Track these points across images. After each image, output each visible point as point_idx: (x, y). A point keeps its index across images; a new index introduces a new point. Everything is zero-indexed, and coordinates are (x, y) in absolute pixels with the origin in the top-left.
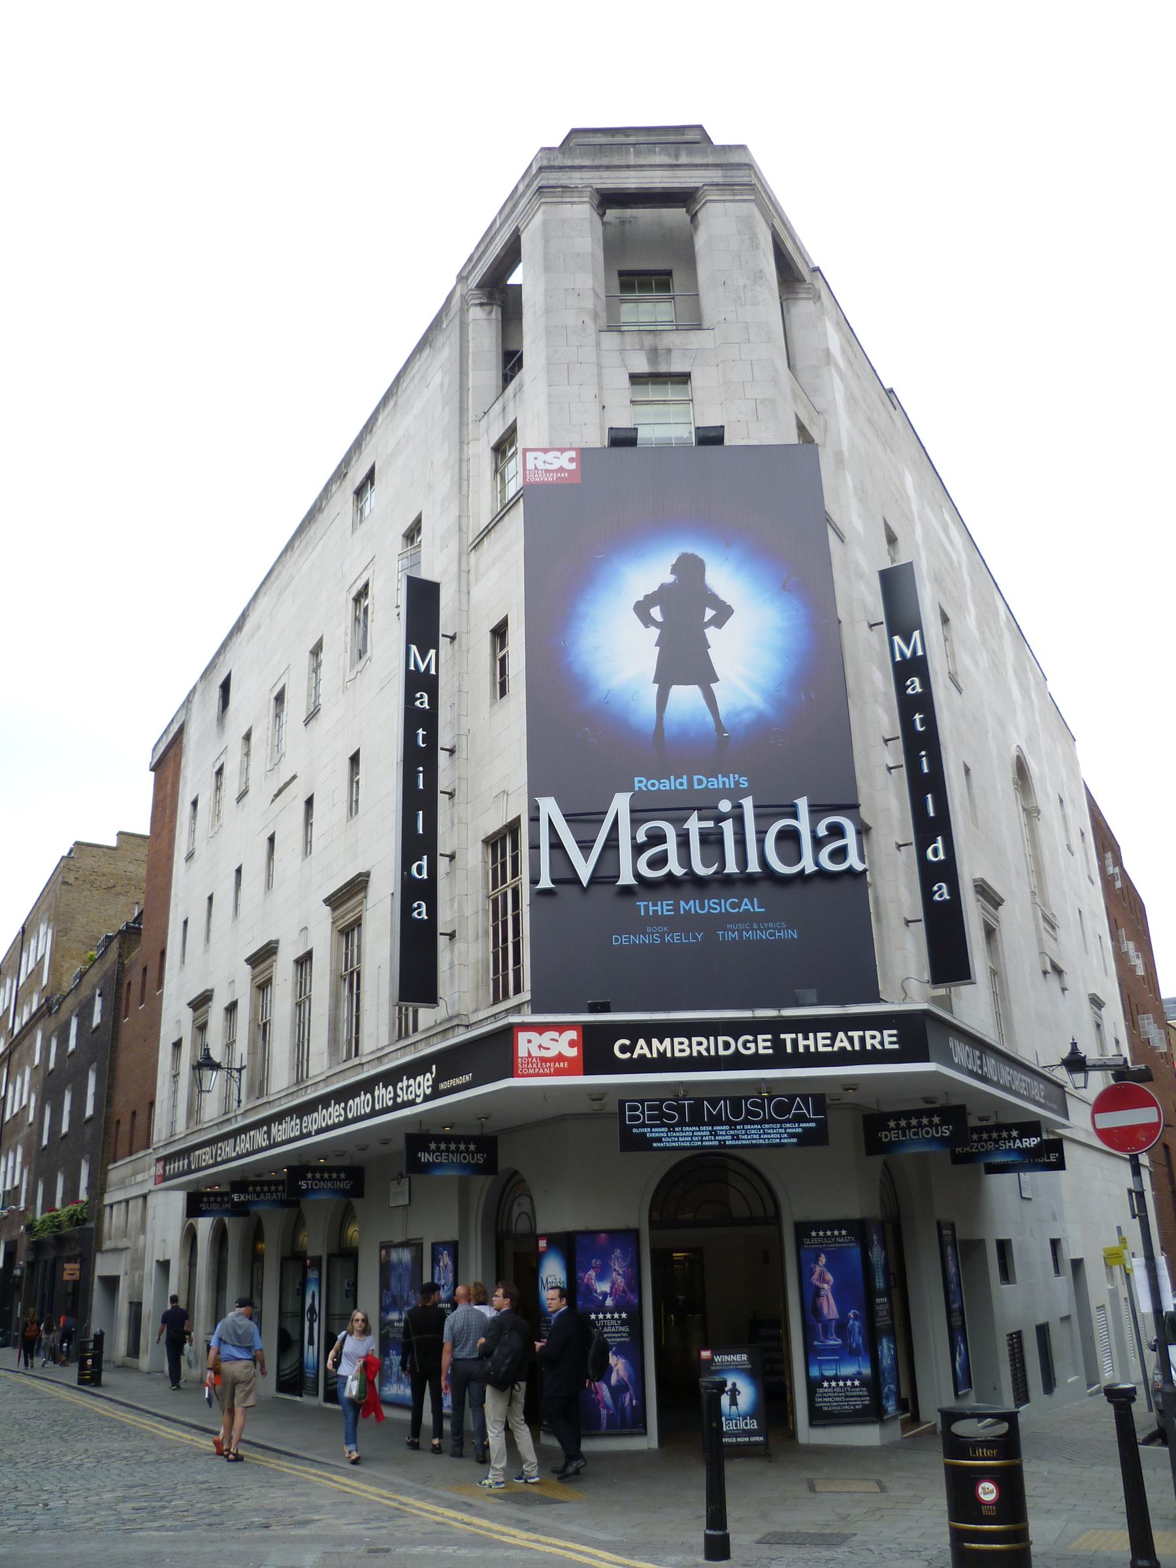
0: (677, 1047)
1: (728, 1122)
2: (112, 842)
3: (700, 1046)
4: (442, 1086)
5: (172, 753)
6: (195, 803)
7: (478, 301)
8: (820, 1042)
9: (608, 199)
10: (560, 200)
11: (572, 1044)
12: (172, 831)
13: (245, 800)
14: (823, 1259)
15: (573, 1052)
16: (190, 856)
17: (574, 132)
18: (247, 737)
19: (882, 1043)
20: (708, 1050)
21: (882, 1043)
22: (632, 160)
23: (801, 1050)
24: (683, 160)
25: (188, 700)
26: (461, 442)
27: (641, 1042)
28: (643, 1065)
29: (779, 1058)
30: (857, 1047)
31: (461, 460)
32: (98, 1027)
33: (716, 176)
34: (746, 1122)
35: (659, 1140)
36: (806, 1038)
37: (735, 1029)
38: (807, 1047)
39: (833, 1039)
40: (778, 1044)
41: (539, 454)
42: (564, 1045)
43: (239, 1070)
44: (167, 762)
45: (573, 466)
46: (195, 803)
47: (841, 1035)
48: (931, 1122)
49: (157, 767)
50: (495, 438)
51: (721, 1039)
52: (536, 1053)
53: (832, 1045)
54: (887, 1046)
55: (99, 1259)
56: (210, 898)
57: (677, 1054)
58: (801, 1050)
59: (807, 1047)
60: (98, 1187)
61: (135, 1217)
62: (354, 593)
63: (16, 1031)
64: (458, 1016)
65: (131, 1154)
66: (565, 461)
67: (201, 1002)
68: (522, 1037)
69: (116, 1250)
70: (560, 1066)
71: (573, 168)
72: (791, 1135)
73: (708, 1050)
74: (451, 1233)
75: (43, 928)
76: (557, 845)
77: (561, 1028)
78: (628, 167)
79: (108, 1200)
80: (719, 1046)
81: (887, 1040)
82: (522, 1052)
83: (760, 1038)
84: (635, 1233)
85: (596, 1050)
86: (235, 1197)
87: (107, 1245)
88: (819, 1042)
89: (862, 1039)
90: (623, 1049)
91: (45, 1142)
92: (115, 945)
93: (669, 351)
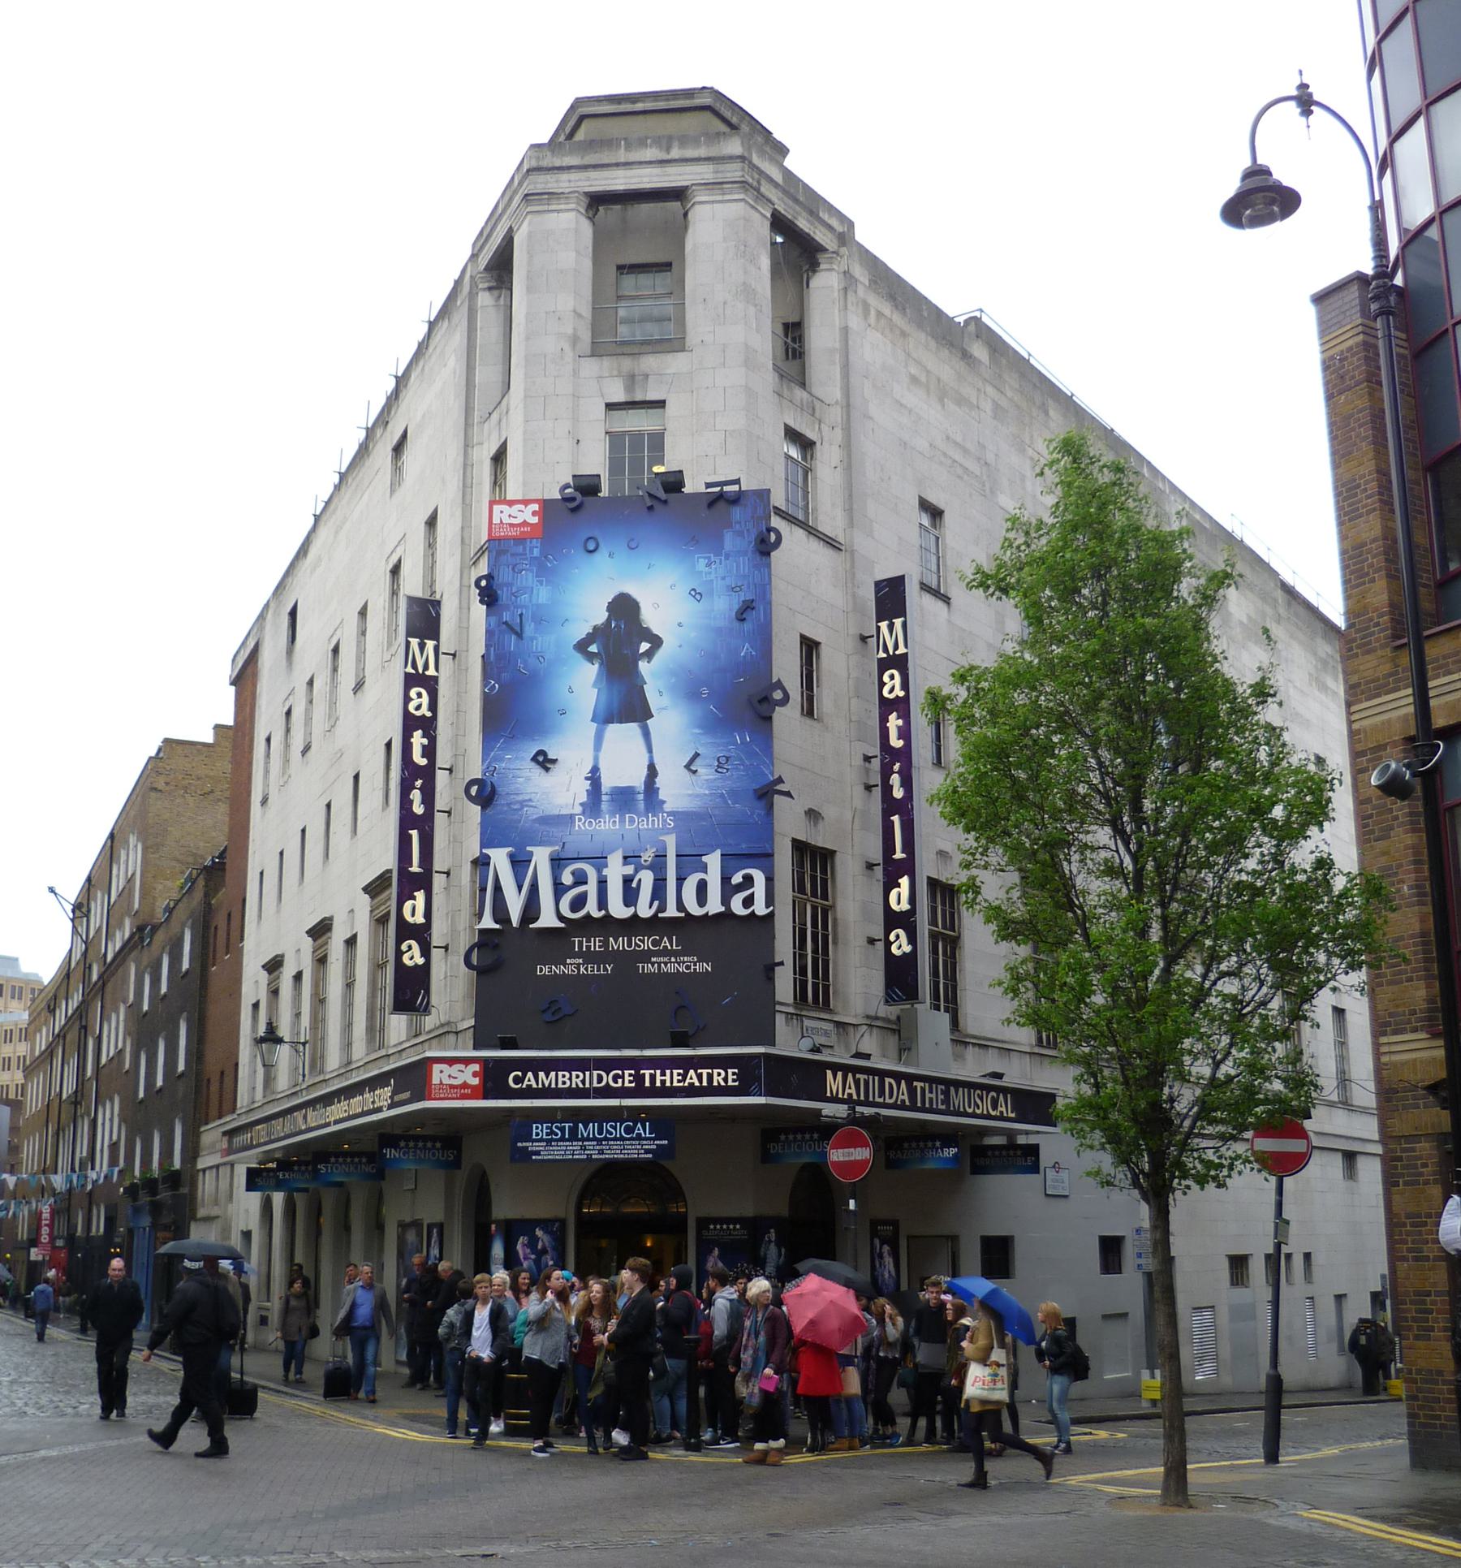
0: (560, 1079)
1: (595, 1139)
2: (208, 737)
3: (576, 1079)
4: (396, 1098)
5: (249, 671)
6: (268, 740)
7: (486, 285)
8: (676, 1078)
9: (597, 201)
10: (545, 208)
11: (475, 1074)
12: (250, 764)
13: (309, 754)
14: (716, 1252)
15: (476, 1081)
16: (264, 801)
17: (578, 102)
18: (311, 683)
19: (726, 1079)
20: (583, 1082)
21: (726, 1079)
22: (622, 156)
23: (658, 1084)
24: (675, 153)
25: (262, 617)
26: (466, 446)
27: (530, 1074)
28: (529, 1093)
29: (639, 1091)
30: (705, 1083)
31: (465, 465)
32: (187, 971)
33: (705, 172)
34: (606, 1139)
35: (538, 1153)
36: (663, 1074)
37: (606, 1065)
38: (663, 1082)
39: (684, 1077)
40: (639, 1079)
41: (504, 507)
42: (468, 1075)
43: (304, 1044)
44: (245, 678)
45: (535, 520)
46: (268, 740)
47: (692, 1072)
48: (812, 1138)
49: (236, 681)
50: (493, 451)
51: (595, 1073)
52: (446, 1081)
53: (684, 1080)
54: (730, 1083)
55: (193, 1226)
56: (281, 853)
57: (560, 1085)
58: (658, 1084)
59: (663, 1082)
60: (192, 1151)
61: (224, 1184)
62: (390, 566)
63: (109, 958)
64: (448, 1023)
65: (220, 1118)
66: (528, 515)
67: (274, 966)
68: (436, 1068)
69: (208, 1219)
70: (464, 1092)
71: (561, 169)
72: (647, 1151)
73: (583, 1082)
74: (439, 1217)
75: (132, 840)
76: (498, 888)
77: (467, 1061)
78: (617, 165)
79: (200, 1165)
80: (592, 1079)
81: (730, 1077)
82: (435, 1080)
83: (627, 1072)
84: (563, 1222)
85: (494, 1079)
86: (280, 1175)
87: (202, 1212)
88: (672, 1078)
89: (710, 1077)
90: (517, 1080)
91: (141, 1095)
92: (201, 882)
93: (647, 376)
